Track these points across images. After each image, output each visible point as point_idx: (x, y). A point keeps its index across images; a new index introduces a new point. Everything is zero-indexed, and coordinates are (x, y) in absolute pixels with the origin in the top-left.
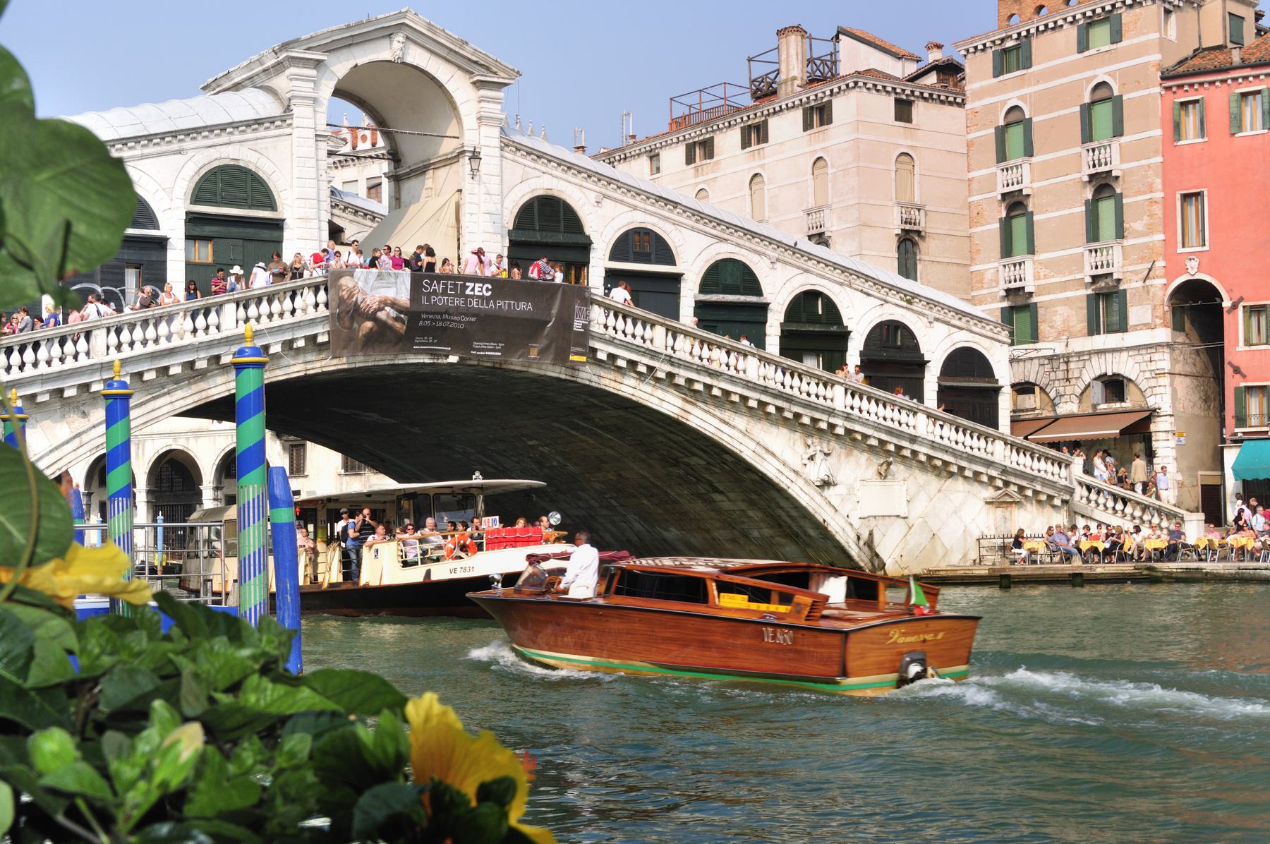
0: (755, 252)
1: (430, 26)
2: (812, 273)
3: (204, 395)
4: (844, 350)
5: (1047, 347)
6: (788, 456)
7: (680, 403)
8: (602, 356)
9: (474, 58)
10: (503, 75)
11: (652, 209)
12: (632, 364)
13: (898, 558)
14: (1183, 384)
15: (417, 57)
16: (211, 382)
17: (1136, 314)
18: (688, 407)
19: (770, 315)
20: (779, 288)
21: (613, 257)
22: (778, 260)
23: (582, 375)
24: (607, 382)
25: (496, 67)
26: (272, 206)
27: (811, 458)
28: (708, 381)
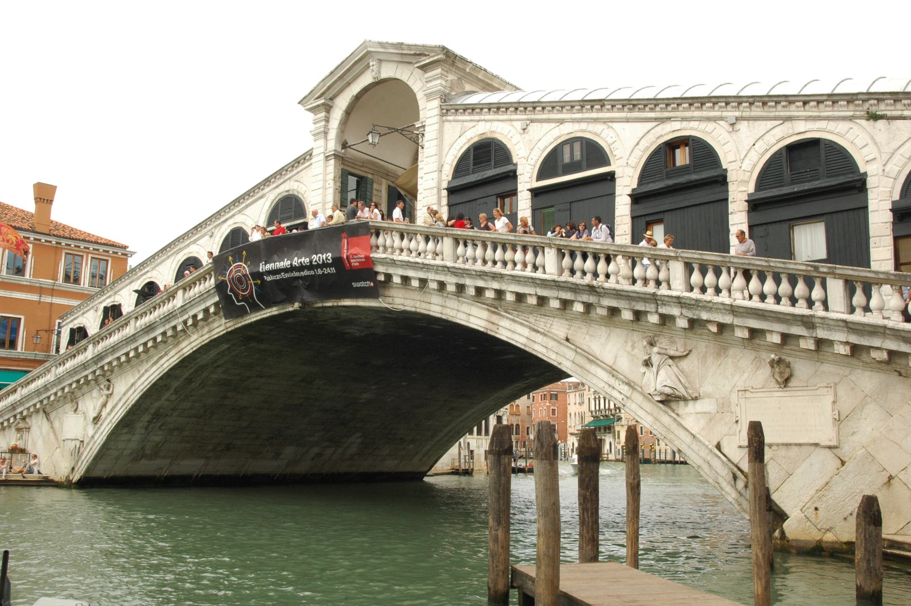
0: (709, 119)
1: (381, 44)
2: (797, 118)
3: (181, 353)
4: (866, 208)
6: (624, 365)
7: (485, 314)
8: (396, 280)
9: (412, 52)
10: (432, 54)
11: (579, 116)
12: (423, 282)
13: (810, 512)
15: (388, 71)
18: (495, 318)
19: (731, 187)
20: (744, 154)
21: (540, 177)
22: (737, 119)
23: (397, 301)
24: (418, 304)
25: (427, 50)
27: (647, 363)
28: (496, 285)
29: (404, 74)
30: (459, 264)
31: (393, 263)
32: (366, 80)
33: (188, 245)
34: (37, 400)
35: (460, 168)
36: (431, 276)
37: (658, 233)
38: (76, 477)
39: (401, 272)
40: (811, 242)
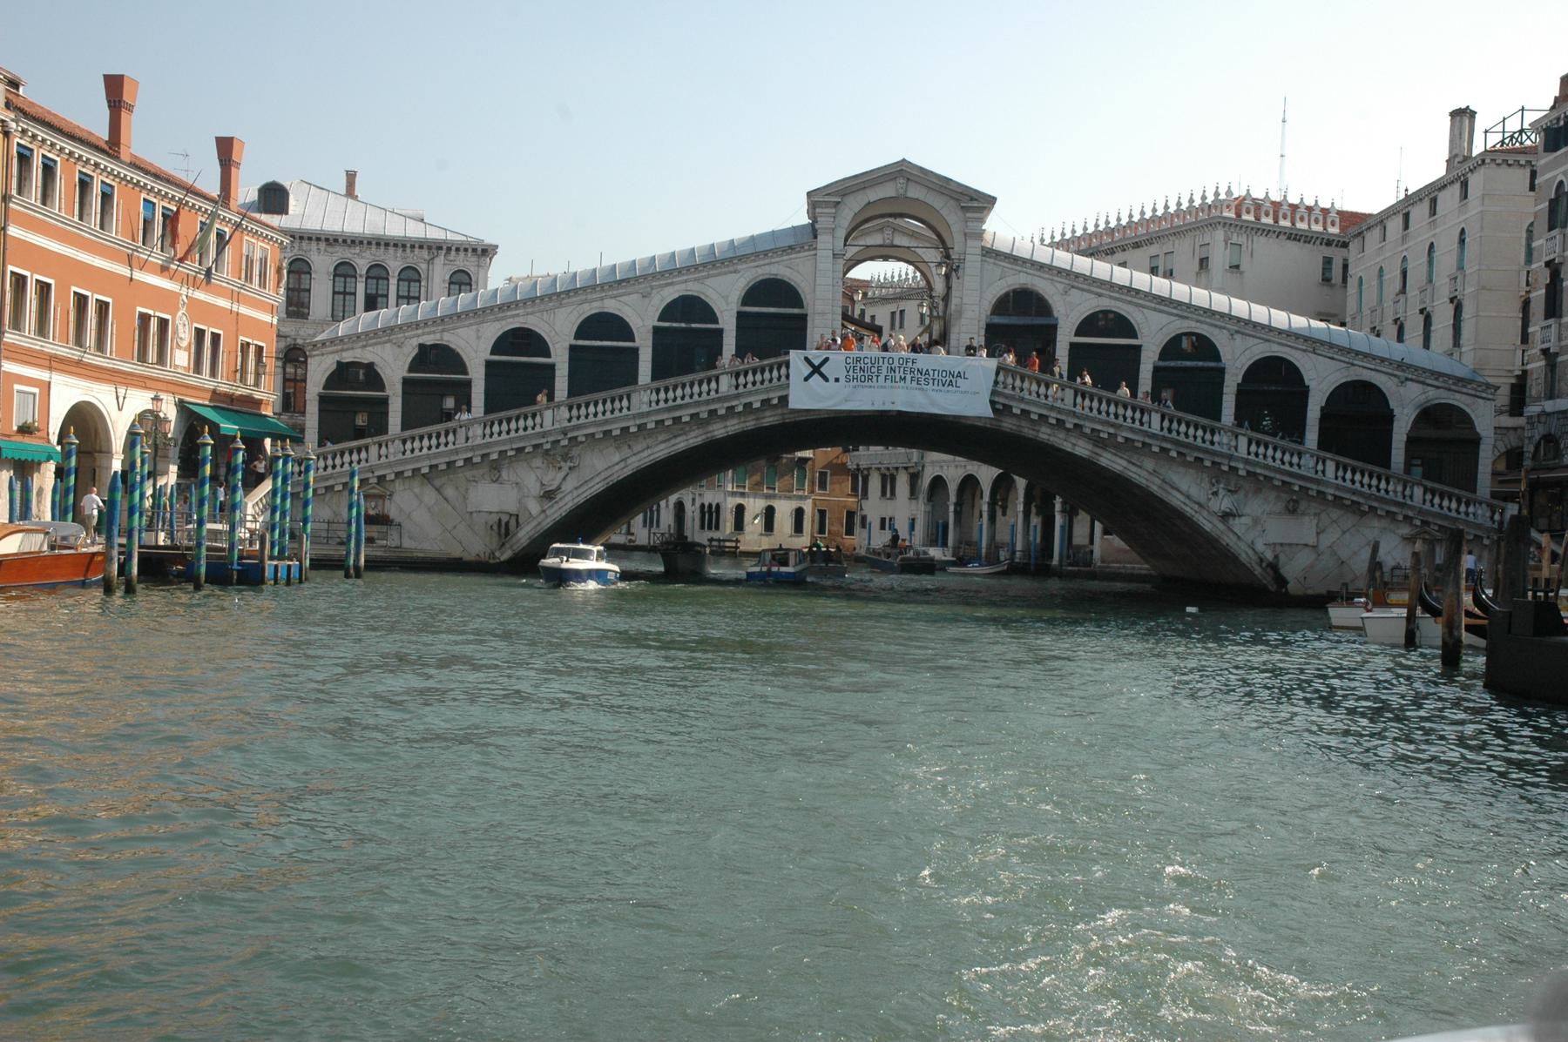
1: (922, 169)
7: (1090, 447)
8: (1017, 411)
15: (914, 192)
16: (715, 427)
19: (1227, 377)
20: (1236, 358)
21: (1078, 334)
26: (801, 305)
28: (1112, 430)
29: (937, 202)
30: (1078, 409)
31: (1022, 400)
32: (888, 191)
33: (602, 299)
34: (428, 463)
35: (1001, 306)
36: (1053, 414)
37: (1167, 394)
38: (506, 555)
39: (1023, 406)
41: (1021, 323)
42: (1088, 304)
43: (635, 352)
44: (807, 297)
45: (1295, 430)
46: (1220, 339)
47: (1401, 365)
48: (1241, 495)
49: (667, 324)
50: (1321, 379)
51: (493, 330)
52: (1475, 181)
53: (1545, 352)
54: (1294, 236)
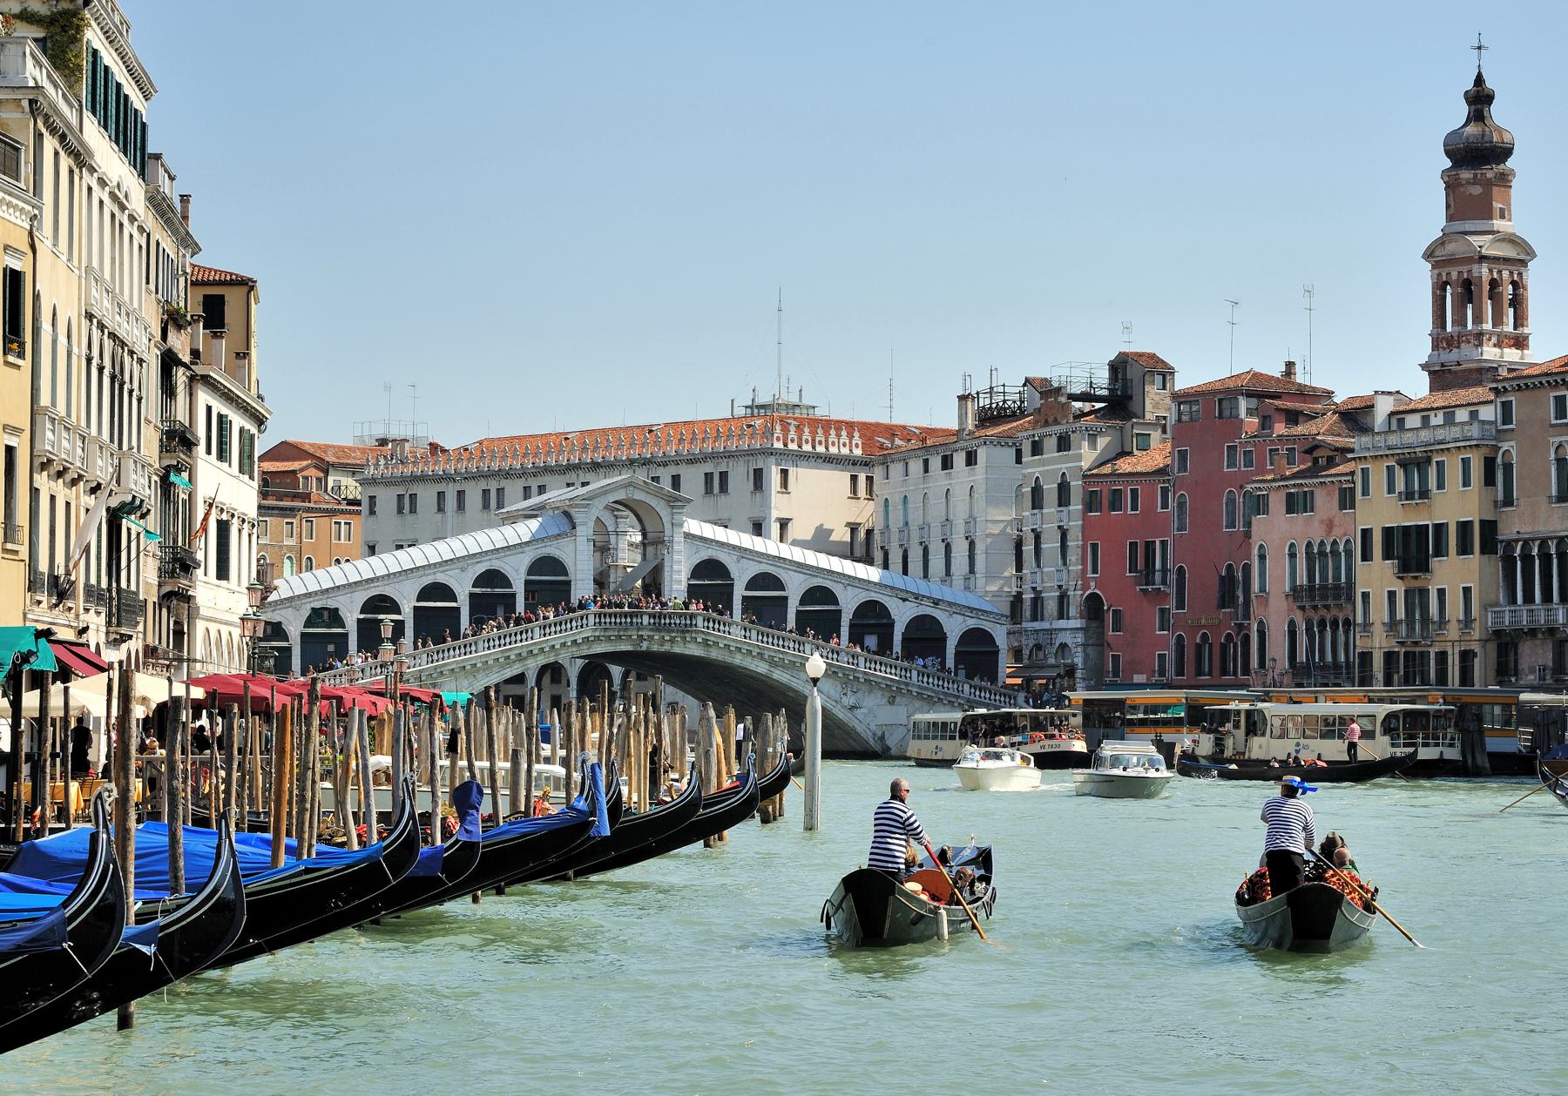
5: (1045, 625)
6: (832, 692)
14: (1090, 650)
15: (639, 496)
17: (1073, 611)
29: (653, 502)
40: (871, 641)
41: (711, 580)
42: (754, 569)
43: (458, 609)
44: (571, 569)
45: (885, 647)
46: (837, 589)
47: (950, 604)
48: (859, 694)
49: (477, 590)
50: (902, 614)
51: (362, 597)
52: (982, 454)
53: (1034, 589)
54: (829, 460)
